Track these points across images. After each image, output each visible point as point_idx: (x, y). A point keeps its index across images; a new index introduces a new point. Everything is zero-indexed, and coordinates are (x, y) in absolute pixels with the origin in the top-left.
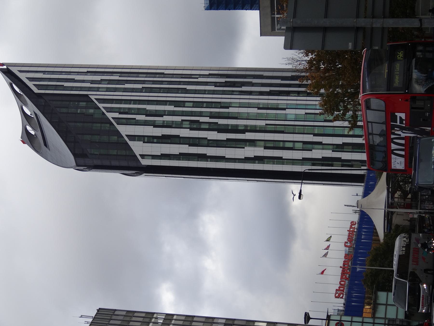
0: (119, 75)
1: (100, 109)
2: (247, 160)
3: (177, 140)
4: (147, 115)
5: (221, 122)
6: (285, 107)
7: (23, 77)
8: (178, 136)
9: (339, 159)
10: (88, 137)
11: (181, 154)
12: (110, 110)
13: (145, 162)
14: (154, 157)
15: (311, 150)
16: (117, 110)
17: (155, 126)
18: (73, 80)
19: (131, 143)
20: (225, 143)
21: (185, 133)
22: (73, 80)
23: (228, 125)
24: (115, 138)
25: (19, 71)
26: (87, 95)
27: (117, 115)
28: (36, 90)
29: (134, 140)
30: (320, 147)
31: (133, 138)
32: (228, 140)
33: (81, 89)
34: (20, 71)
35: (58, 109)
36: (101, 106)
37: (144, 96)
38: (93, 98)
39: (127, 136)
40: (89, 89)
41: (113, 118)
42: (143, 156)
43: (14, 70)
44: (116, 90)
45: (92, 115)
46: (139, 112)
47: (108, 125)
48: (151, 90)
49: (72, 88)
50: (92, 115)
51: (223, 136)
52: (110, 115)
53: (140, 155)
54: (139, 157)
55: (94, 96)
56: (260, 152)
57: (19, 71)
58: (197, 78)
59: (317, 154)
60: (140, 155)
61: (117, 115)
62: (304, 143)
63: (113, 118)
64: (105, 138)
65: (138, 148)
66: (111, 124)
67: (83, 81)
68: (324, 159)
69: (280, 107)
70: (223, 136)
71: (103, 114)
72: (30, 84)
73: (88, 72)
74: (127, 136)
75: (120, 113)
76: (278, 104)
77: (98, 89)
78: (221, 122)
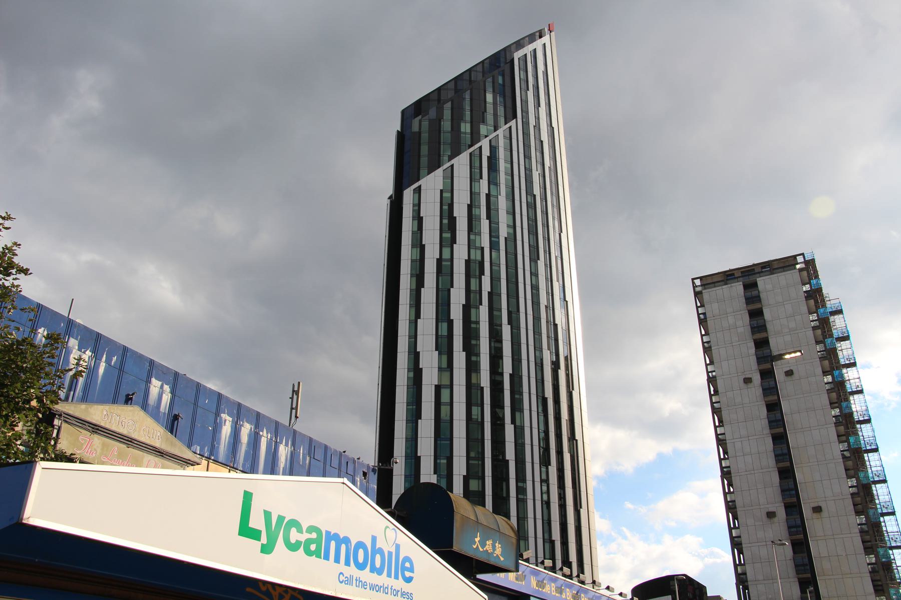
2: (415, 356)
6: (518, 423)
8: (453, 240)
10: (447, 114)
11: (422, 248)
12: (493, 149)
13: (408, 195)
14: (417, 206)
15: (435, 473)
17: (470, 207)
19: (439, 172)
21: (461, 252)
26: (515, 116)
31: (450, 175)
36: (500, 132)
38: (513, 123)
40: (526, 124)
41: (480, 148)
42: (418, 190)
44: (527, 156)
48: (532, 206)
50: (483, 122)
53: (420, 187)
60: (420, 187)
61: (486, 153)
62: (450, 460)
65: (431, 184)
66: (470, 146)
69: (518, 415)
70: (456, 314)
74: (452, 166)
77: (526, 134)
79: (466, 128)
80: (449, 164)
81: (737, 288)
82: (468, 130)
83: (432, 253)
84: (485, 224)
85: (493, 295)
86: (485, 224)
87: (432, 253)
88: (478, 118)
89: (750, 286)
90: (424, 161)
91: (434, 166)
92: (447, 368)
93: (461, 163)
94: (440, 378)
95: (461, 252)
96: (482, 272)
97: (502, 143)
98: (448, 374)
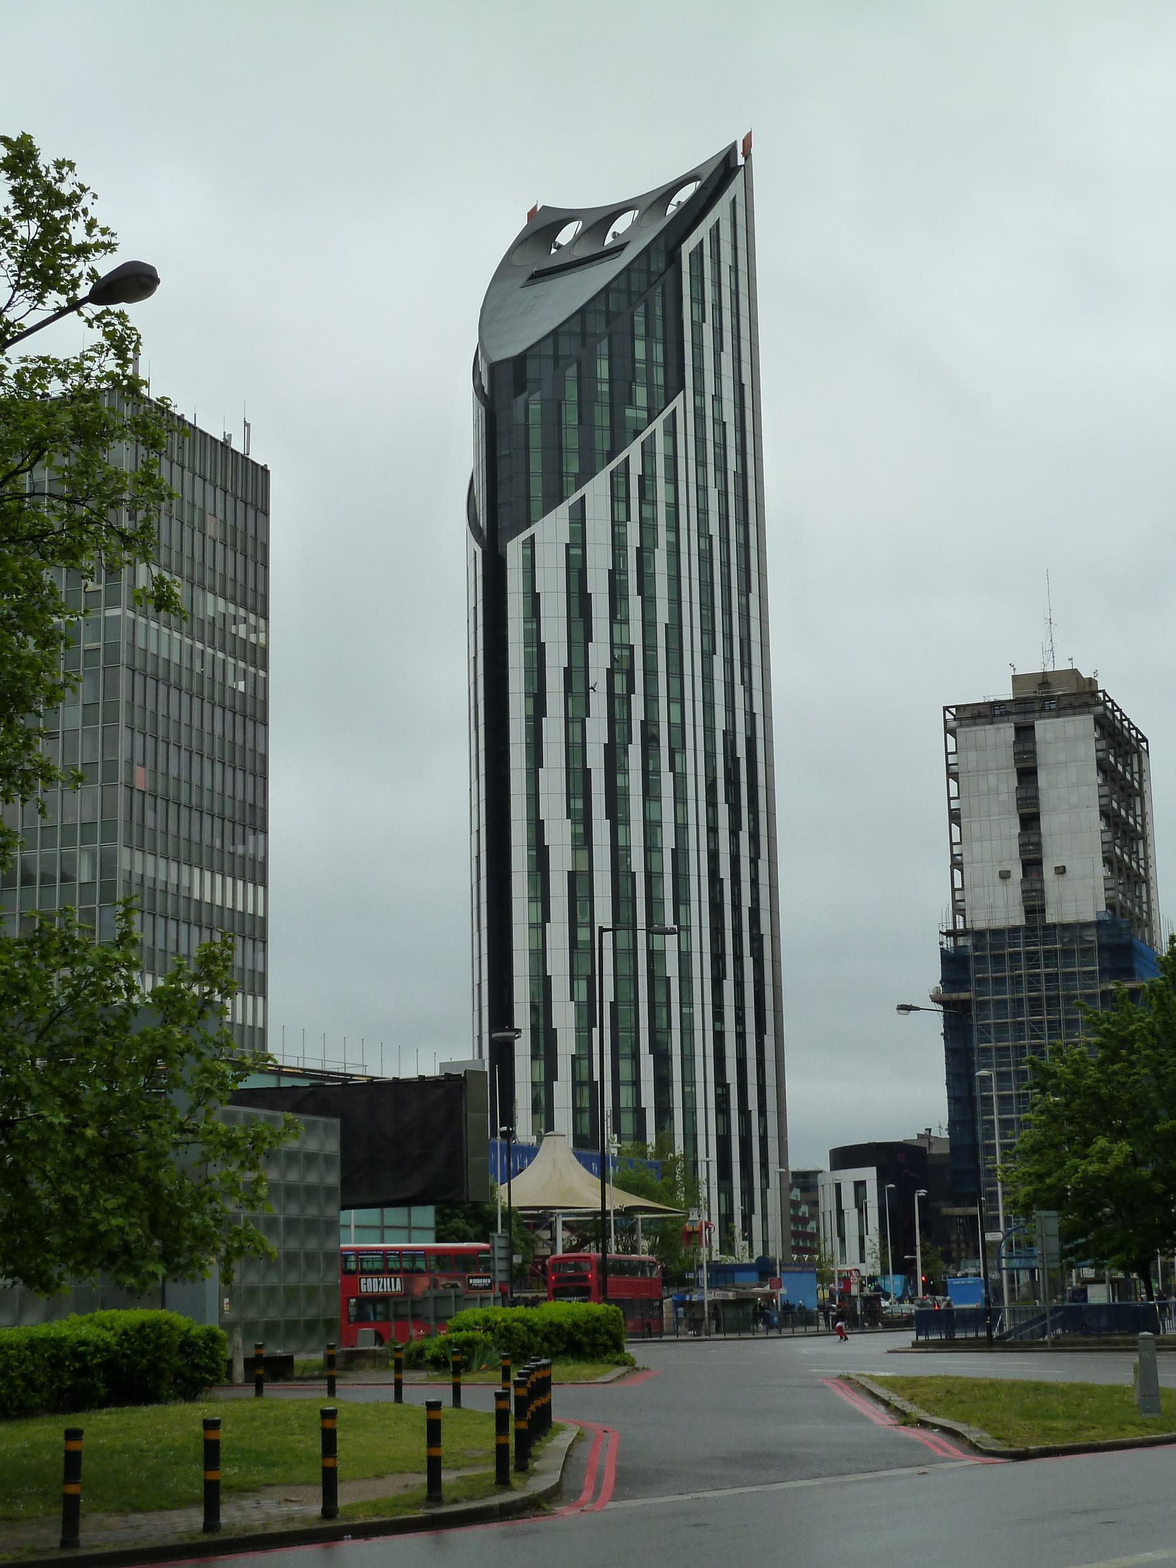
0: (740, 471)
1: (650, 420)
2: (537, 827)
3: (579, 635)
4: (640, 551)
5: (635, 751)
7: (720, 211)
8: (588, 637)
9: (551, 1074)
10: (572, 393)
11: (541, 647)
12: (648, 452)
13: (514, 551)
15: (572, 999)
16: (648, 470)
17: (612, 574)
18: (718, 348)
19: (562, 511)
20: (578, 765)
21: (599, 656)
22: (718, 348)
23: (626, 772)
24: (573, 466)
25: (734, 199)
26: (682, 386)
27: (636, 469)
28: (687, 247)
29: (571, 520)
30: (584, 1023)
31: (579, 515)
32: (587, 773)
33: (699, 371)
34: (734, 202)
35: (641, 309)
36: (658, 425)
37: (690, 545)
38: (678, 402)
39: (583, 498)
40: (699, 392)
41: (627, 459)
43: (735, 187)
44: (701, 463)
45: (631, 404)
46: (648, 527)
47: (607, 447)
48: (706, 558)
49: (698, 346)
50: (631, 404)
51: (596, 760)
52: (633, 451)
53: (532, 537)
54: (525, 535)
55: (682, 404)
56: (561, 861)
57: (734, 199)
58: (743, 683)
59: (564, 1016)
60: (532, 537)
61: (636, 469)
63: (627, 459)
64: (572, 439)
65: (551, 530)
66: (611, 456)
67: (718, 375)
68: (551, 1035)
69: (682, 908)
70: (596, 760)
71: (637, 433)
72: (702, 232)
73: (742, 386)
74: (583, 498)
75: (641, 479)
76: (687, 903)
78: (635, 751)
79: (602, 417)
80: (574, 498)
81: (1006, 732)
82: (607, 422)
83: (556, 659)
84: (635, 603)
85: (649, 725)
86: (635, 603)
87: (556, 659)
88: (621, 397)
89: (1025, 733)
90: (536, 490)
91: (553, 499)
92: (583, 841)
93: (597, 492)
94: (575, 861)
95: (599, 656)
96: (631, 689)
97: (661, 447)
98: (585, 853)
